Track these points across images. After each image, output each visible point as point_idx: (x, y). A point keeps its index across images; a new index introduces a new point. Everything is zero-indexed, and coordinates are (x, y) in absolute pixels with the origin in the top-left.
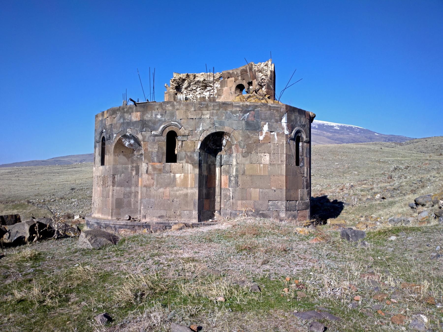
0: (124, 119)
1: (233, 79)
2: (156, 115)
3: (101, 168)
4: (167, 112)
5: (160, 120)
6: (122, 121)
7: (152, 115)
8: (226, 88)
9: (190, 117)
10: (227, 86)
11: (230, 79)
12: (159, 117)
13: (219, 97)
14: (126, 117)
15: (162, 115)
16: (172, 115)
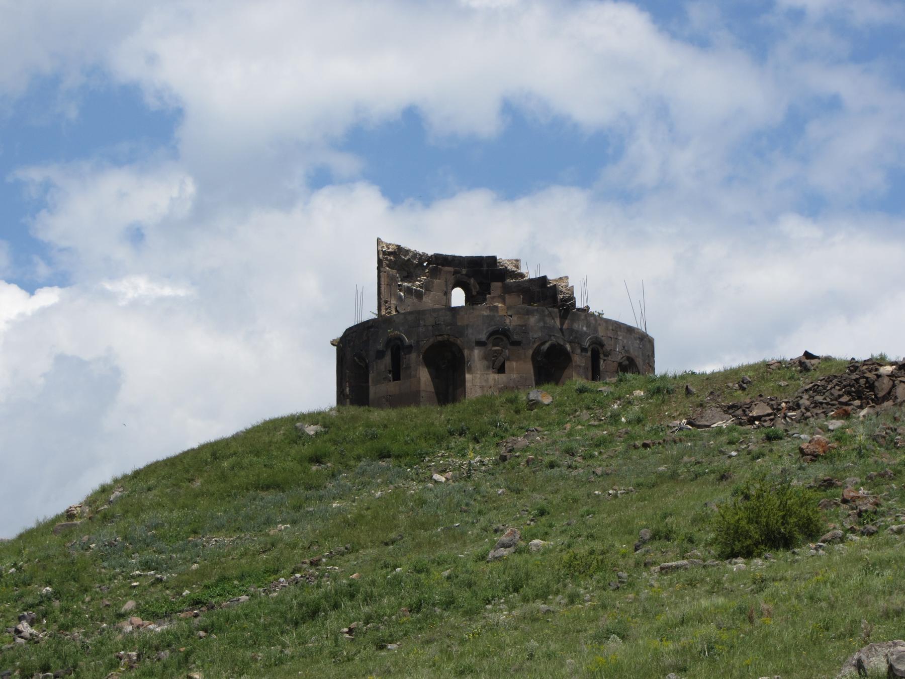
0: (545, 323)
1: (451, 269)
2: (583, 326)
3: (496, 376)
4: (592, 325)
5: (585, 333)
6: (542, 324)
7: (579, 326)
8: (437, 280)
9: (609, 335)
10: (439, 279)
11: (447, 269)
12: (585, 329)
13: (427, 292)
14: (548, 322)
15: (587, 327)
16: (596, 330)
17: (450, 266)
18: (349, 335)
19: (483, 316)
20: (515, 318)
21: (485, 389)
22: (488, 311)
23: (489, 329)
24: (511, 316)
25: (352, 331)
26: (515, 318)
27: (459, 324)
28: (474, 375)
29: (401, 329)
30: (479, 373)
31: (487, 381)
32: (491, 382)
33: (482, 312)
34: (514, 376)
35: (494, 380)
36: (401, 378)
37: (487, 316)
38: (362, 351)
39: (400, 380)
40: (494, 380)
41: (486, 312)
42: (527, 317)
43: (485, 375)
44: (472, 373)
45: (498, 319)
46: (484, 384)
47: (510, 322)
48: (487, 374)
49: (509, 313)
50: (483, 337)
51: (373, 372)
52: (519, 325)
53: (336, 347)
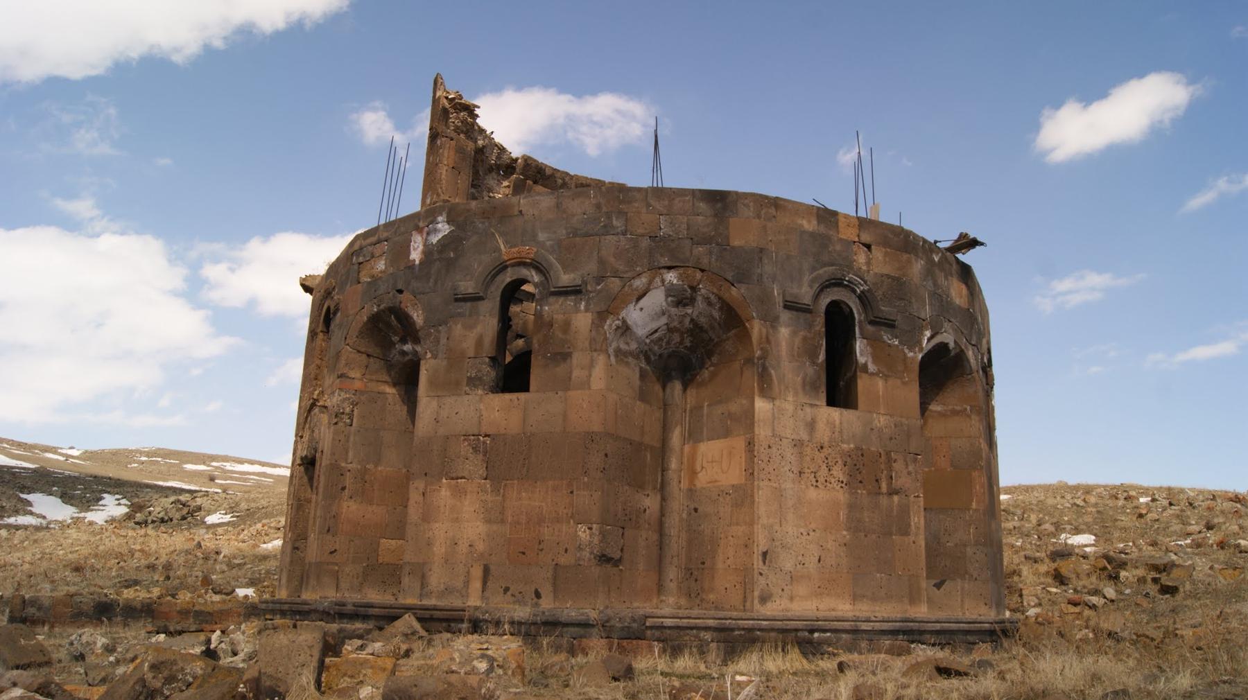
0: (935, 284)
3: (835, 413)
17: (545, 187)
18: (361, 248)
19: (803, 232)
20: (877, 253)
21: (808, 450)
22: (815, 222)
23: (821, 271)
24: (868, 247)
25: (373, 239)
26: (877, 253)
27: (736, 242)
28: (777, 403)
29: (542, 236)
30: (790, 398)
31: (811, 426)
32: (823, 434)
33: (800, 221)
34: (881, 421)
35: (830, 424)
36: (532, 388)
37: (813, 235)
38: (400, 292)
39: (525, 388)
40: (830, 424)
41: (809, 222)
42: (905, 256)
43: (808, 410)
44: (773, 399)
45: (838, 248)
46: (804, 436)
47: (868, 263)
48: (812, 405)
49: (866, 238)
50: (805, 293)
51: (435, 357)
52: (888, 276)
53: (308, 298)
